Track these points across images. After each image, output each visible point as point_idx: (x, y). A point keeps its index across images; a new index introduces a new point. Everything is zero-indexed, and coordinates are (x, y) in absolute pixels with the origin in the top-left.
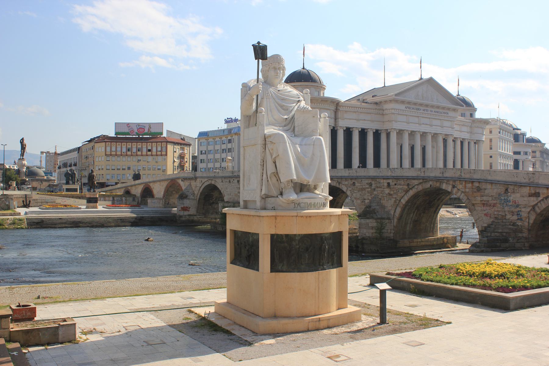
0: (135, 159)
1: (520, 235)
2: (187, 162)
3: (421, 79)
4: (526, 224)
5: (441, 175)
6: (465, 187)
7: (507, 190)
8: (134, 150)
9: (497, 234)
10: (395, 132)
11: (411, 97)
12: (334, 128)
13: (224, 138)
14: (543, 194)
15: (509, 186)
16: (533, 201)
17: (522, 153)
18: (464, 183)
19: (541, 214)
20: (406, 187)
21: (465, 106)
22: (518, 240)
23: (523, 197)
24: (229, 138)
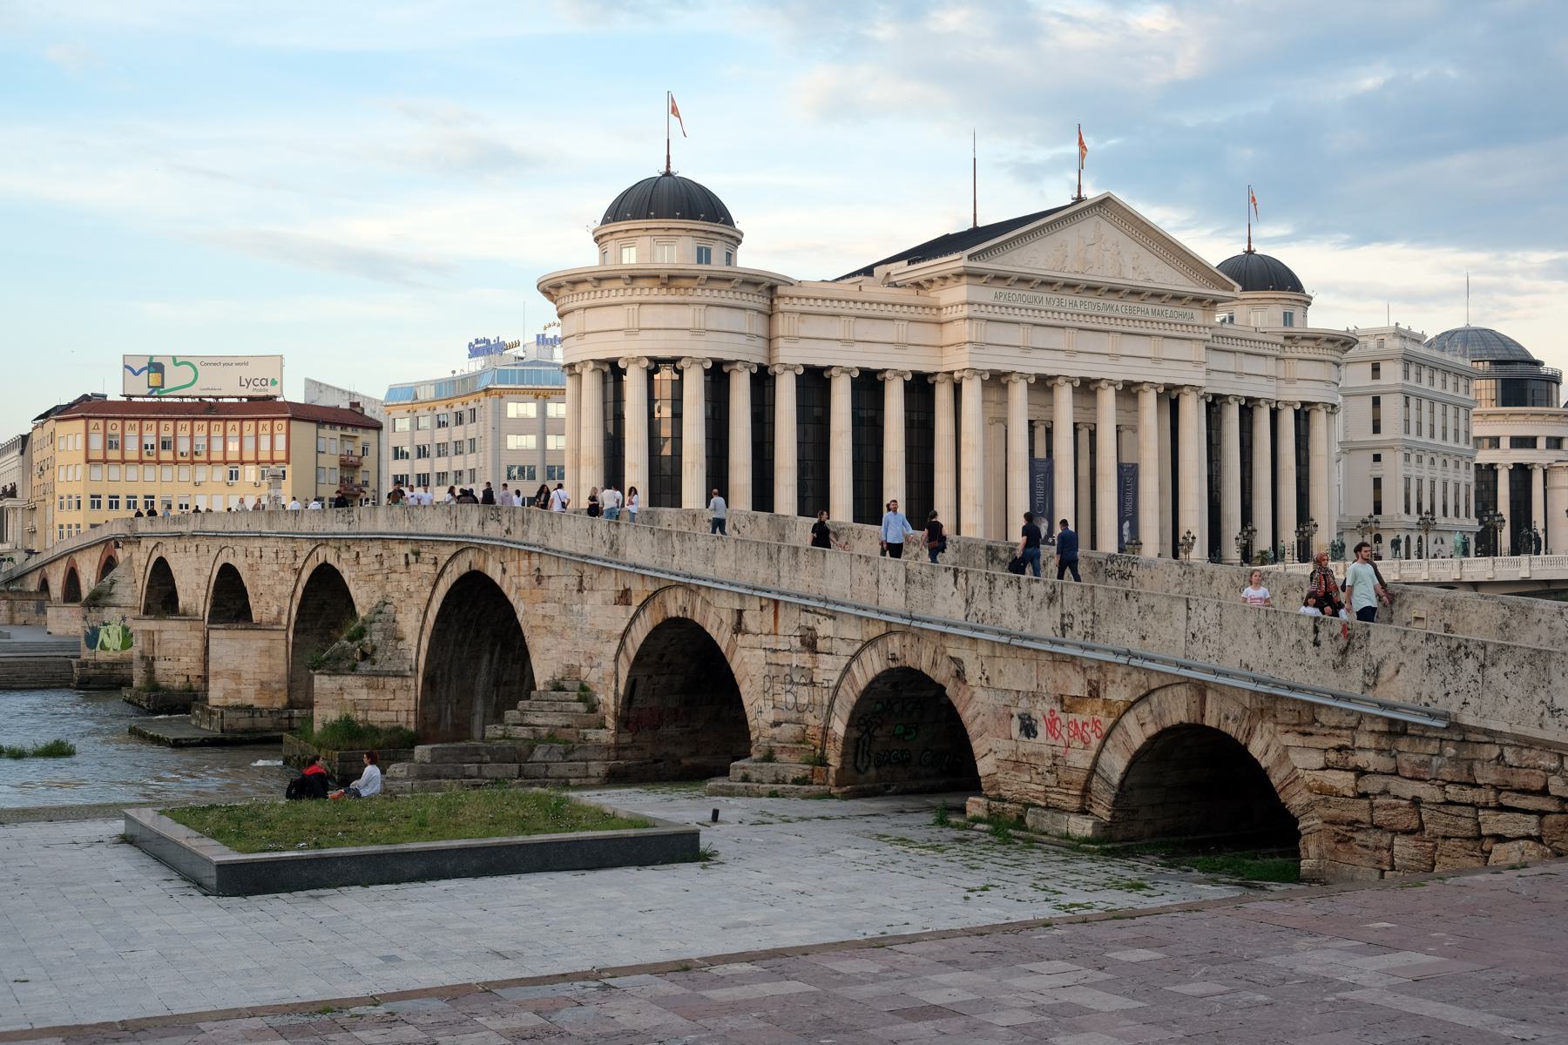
0: (185, 472)
1: (592, 735)
2: (366, 484)
3: (1079, 199)
4: (611, 695)
5: (477, 531)
8: (184, 446)
10: (977, 382)
11: (1034, 258)
12: (763, 369)
13: (441, 409)
16: (622, 615)
17: (1541, 443)
20: (431, 569)
21: (1238, 287)
24: (472, 405)
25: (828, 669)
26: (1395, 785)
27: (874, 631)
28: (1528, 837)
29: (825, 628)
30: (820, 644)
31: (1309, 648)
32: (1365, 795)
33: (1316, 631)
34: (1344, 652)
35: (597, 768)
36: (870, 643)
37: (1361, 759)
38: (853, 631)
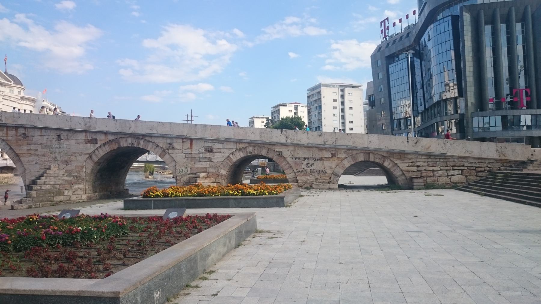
6: (7, 134)
7: (59, 136)
9: (48, 187)
14: (101, 140)
15: (62, 132)
16: (90, 148)
18: (5, 129)
19: (98, 163)
21: (13, 82)
22: (74, 192)
23: (79, 144)
25: (218, 158)
26: (428, 168)
27: (242, 146)
28: (459, 174)
29: (216, 146)
30: (214, 151)
31: (406, 143)
32: (420, 171)
33: (408, 139)
34: (416, 143)
35: (84, 197)
36: (240, 150)
37: (418, 164)
38: (232, 147)
